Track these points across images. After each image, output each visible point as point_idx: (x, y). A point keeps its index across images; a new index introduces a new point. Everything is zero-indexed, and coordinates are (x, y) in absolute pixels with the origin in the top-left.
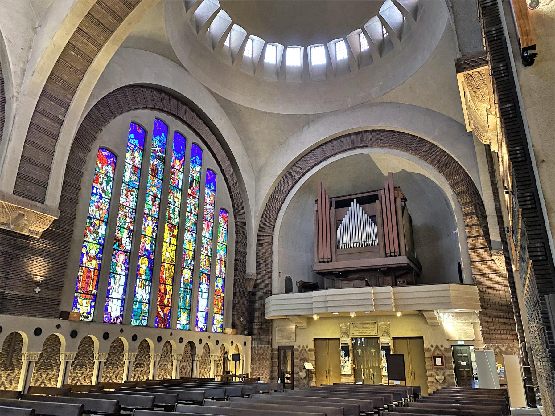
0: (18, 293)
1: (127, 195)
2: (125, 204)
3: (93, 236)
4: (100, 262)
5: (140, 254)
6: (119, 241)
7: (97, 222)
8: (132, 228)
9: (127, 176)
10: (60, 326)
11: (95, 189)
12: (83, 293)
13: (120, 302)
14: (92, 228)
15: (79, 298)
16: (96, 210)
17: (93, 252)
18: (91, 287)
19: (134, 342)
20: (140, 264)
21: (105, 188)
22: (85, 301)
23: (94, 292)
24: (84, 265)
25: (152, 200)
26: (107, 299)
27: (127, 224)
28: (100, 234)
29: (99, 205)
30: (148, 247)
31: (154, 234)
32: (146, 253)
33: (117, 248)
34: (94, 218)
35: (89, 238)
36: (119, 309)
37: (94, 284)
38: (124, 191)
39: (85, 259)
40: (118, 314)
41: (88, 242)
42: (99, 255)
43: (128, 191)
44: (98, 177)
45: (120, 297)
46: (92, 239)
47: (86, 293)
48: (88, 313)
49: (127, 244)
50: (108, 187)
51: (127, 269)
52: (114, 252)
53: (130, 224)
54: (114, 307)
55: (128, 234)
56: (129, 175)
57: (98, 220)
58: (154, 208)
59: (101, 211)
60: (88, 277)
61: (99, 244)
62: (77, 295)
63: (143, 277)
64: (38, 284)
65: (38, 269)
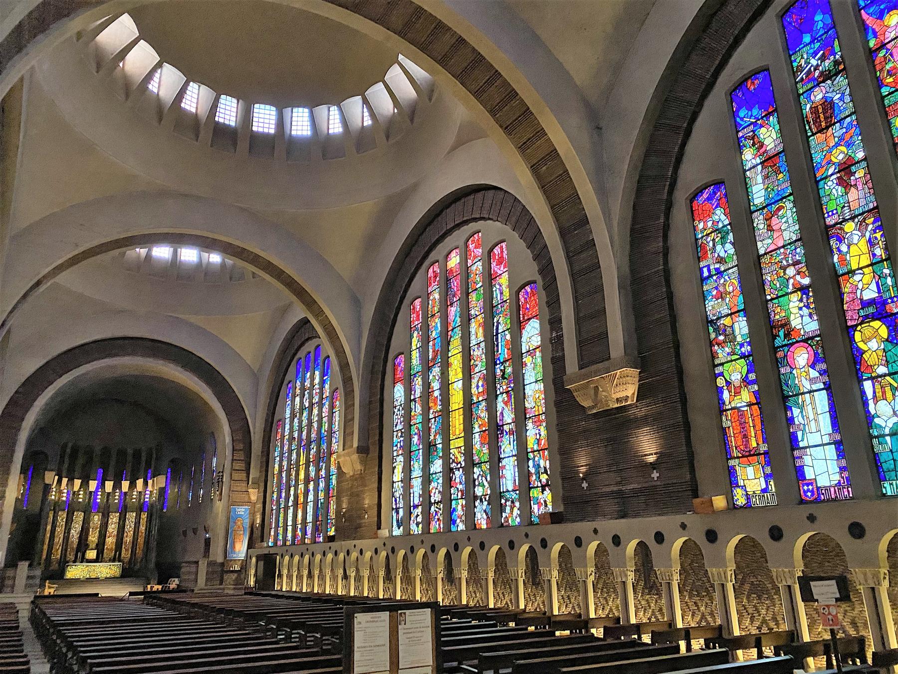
0: (636, 486)
1: (770, 228)
2: (773, 247)
3: (727, 350)
4: (756, 387)
5: (849, 323)
6: (783, 326)
7: (727, 321)
8: (806, 281)
9: (758, 194)
10: (808, 518)
11: (705, 270)
12: (743, 457)
13: (831, 451)
14: (721, 338)
15: (737, 468)
16: (723, 302)
17: (736, 378)
18: (753, 440)
19: (715, 545)
20: (862, 345)
21: (722, 254)
22: (750, 470)
23: (764, 448)
24: (727, 407)
25: (841, 182)
26: (796, 453)
27: (791, 281)
28: (739, 339)
29: (721, 289)
30: (870, 294)
31: (878, 252)
32: (871, 310)
33: (786, 342)
34: (718, 319)
35: (722, 354)
36: (834, 467)
37: (759, 432)
38: (761, 226)
39: (726, 395)
40: (836, 478)
41: (722, 364)
42: (750, 375)
43: (768, 219)
44: (703, 247)
45: (826, 439)
46: (728, 354)
47: (749, 455)
48: (764, 491)
49: (807, 319)
50: (728, 246)
51: (822, 373)
52: (780, 354)
53: (798, 278)
54: (820, 466)
55: (801, 300)
56: (761, 186)
57: (727, 316)
58: (853, 194)
59: (727, 300)
60: (743, 425)
61: (743, 356)
62: (732, 463)
63: (882, 370)
64: (653, 466)
65: (648, 445)
